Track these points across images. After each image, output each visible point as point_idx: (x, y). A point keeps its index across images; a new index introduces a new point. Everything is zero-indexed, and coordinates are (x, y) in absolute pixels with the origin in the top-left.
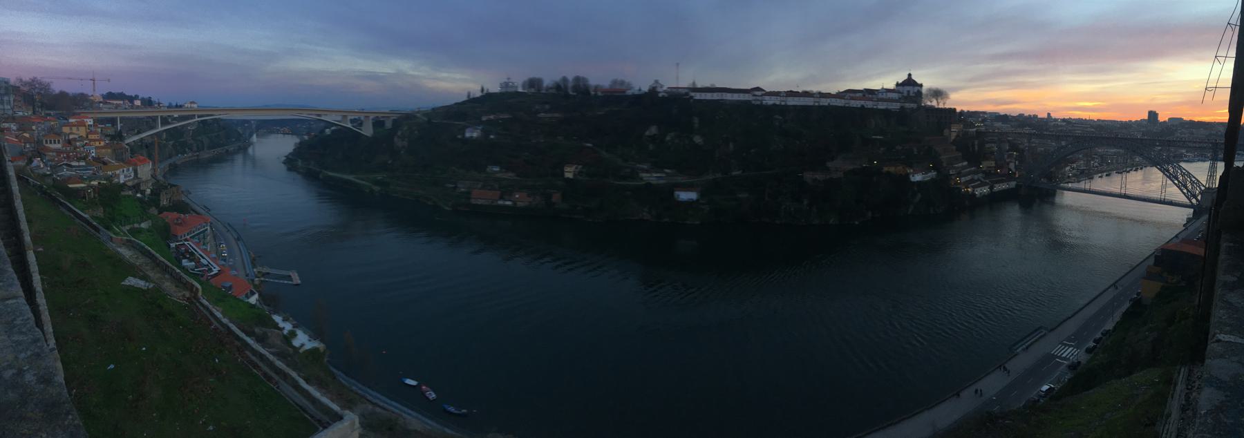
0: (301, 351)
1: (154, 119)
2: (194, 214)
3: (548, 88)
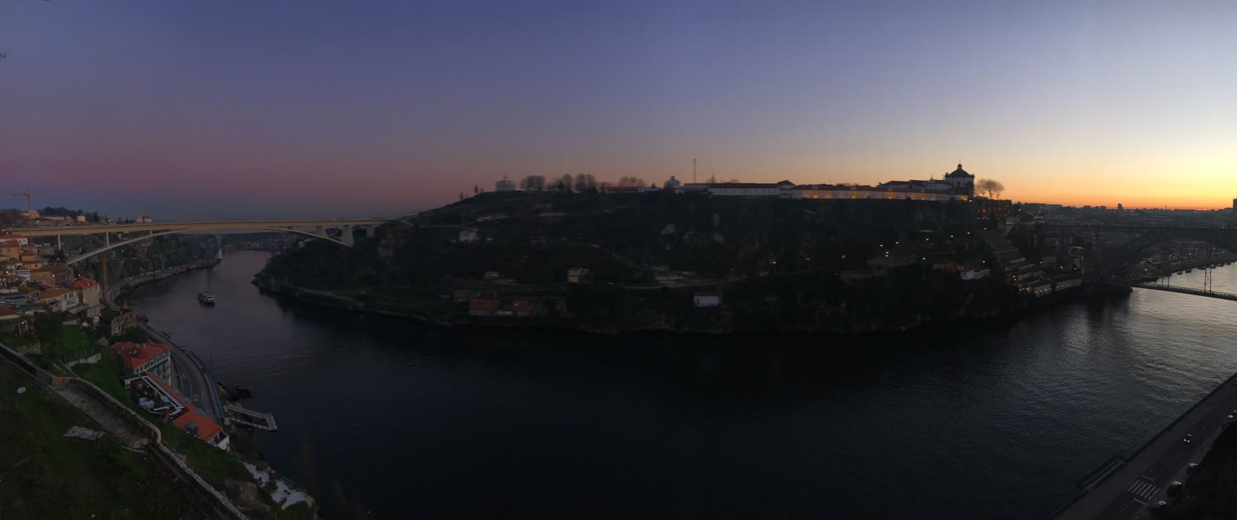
0: (284, 508)
1: (102, 236)
2: (152, 343)
3: (550, 187)
